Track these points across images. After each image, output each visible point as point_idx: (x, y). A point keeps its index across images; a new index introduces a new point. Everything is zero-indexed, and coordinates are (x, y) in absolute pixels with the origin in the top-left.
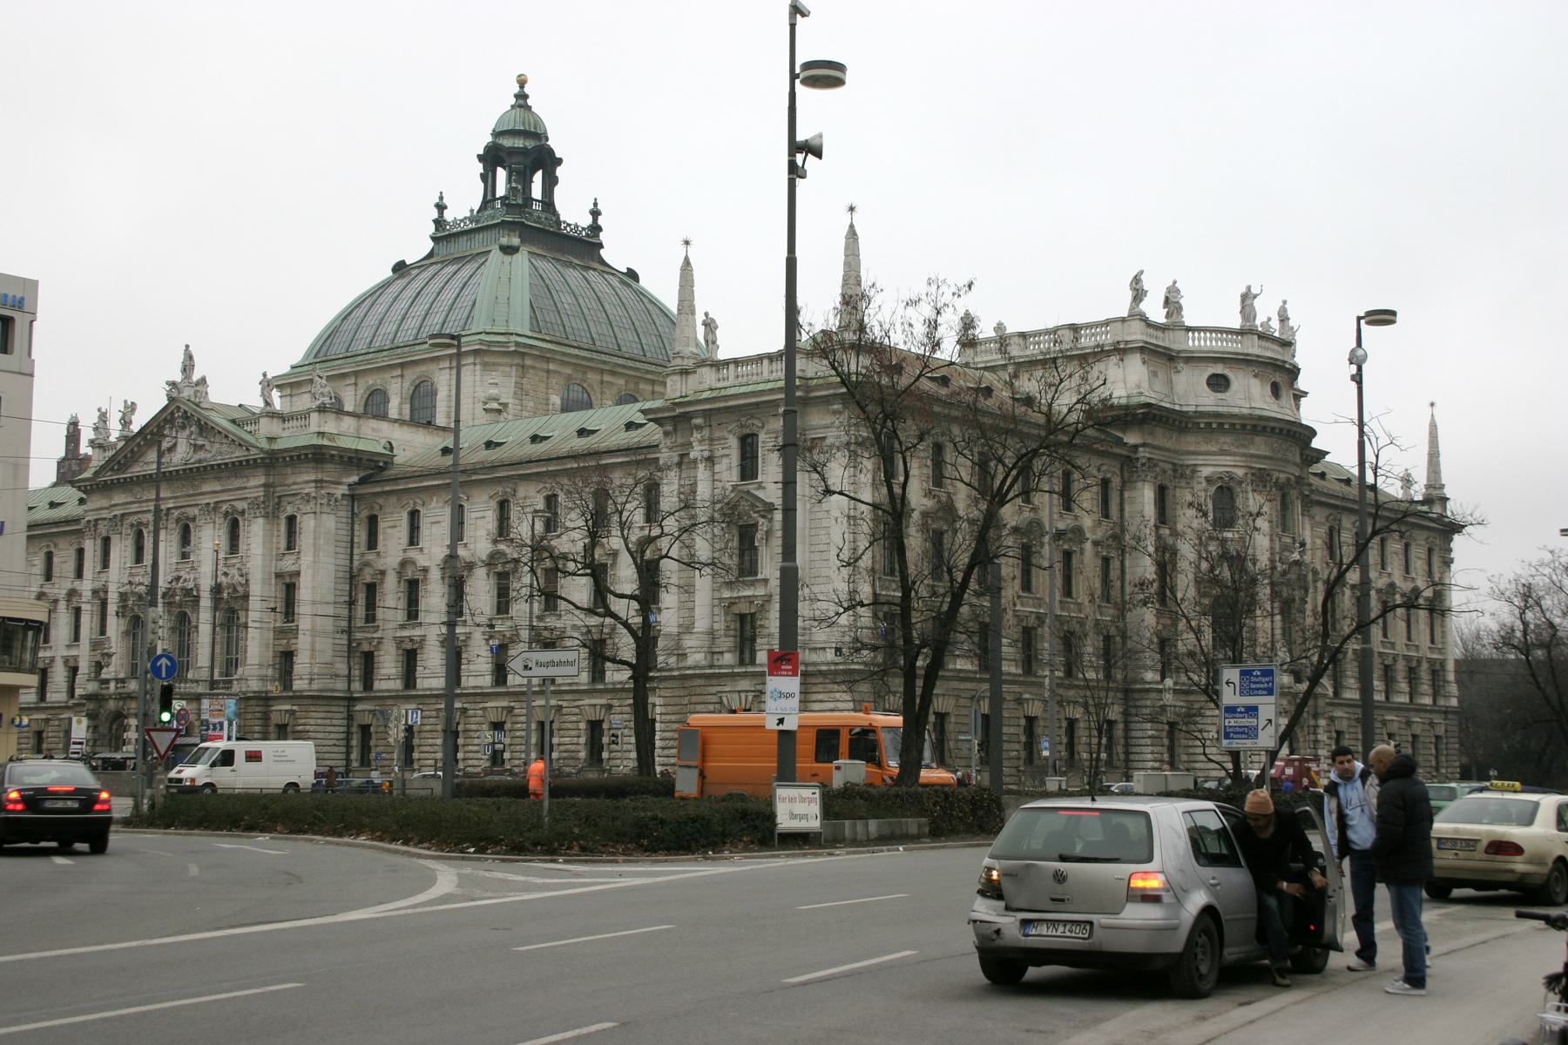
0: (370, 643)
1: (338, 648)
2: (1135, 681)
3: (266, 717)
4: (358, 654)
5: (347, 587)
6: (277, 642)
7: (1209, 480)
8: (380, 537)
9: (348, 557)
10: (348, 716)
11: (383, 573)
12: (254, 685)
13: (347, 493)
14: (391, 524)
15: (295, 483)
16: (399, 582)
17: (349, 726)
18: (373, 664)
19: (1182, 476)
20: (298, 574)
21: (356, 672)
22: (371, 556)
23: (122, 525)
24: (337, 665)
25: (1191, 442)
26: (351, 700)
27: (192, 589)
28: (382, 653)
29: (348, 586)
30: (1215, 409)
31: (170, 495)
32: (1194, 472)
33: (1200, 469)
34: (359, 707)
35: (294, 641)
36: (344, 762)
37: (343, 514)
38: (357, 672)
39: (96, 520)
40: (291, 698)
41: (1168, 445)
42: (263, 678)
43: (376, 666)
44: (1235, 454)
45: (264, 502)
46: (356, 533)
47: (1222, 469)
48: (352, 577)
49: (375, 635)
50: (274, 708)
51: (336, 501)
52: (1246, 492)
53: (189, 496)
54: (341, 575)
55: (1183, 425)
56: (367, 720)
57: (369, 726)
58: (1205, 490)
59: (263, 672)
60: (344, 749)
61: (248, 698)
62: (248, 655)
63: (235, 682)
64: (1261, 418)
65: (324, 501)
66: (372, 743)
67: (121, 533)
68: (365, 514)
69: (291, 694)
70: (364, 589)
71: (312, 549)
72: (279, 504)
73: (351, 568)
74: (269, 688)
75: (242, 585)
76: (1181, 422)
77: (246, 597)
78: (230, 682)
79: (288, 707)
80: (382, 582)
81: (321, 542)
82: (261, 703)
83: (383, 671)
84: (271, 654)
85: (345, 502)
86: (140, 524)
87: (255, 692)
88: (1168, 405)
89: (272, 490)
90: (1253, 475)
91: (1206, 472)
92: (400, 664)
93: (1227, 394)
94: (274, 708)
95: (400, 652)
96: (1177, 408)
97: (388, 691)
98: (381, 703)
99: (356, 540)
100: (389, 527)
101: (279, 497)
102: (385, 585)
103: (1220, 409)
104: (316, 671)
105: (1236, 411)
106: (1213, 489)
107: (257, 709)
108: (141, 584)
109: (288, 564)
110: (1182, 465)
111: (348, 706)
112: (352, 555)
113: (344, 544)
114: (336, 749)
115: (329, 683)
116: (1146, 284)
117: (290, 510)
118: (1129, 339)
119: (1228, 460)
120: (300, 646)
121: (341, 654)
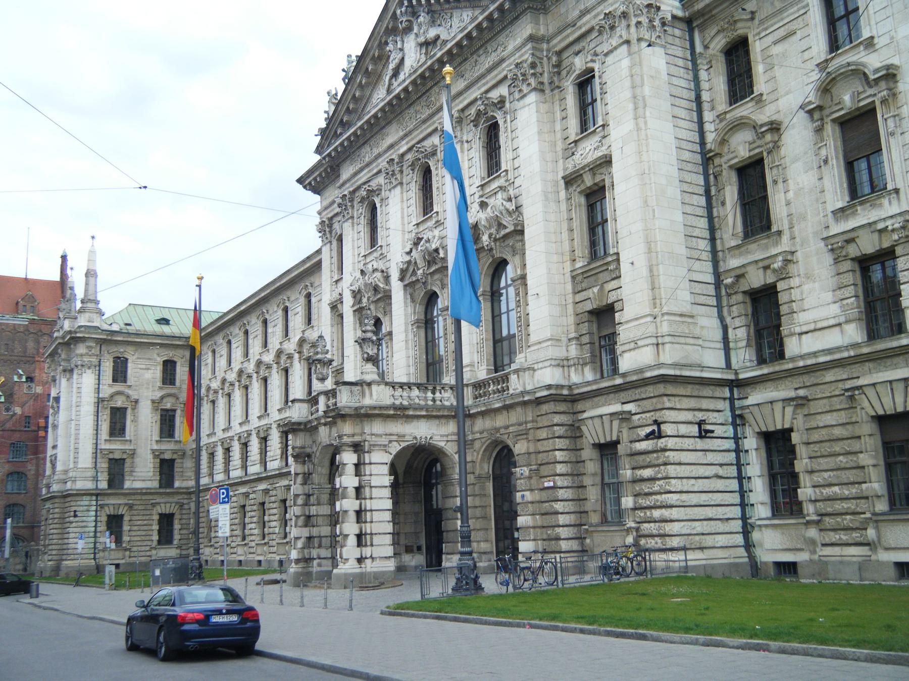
0: (766, 268)
1: (698, 288)
3: (575, 432)
4: (740, 297)
5: (701, 180)
6: (579, 297)
8: (759, 69)
9: (695, 127)
10: (734, 416)
11: (775, 127)
12: (548, 376)
13: (680, 13)
14: (781, 33)
15: (583, 14)
16: (819, 130)
17: (736, 439)
18: (777, 305)
20: (606, 161)
21: (740, 333)
22: (745, 109)
23: (353, 207)
24: (704, 321)
26: (736, 384)
27: (436, 250)
28: (795, 282)
29: (702, 177)
31: (401, 133)
34: (755, 397)
35: (613, 284)
36: (737, 512)
37: (679, 52)
38: (742, 333)
39: (331, 219)
40: (618, 389)
42: (563, 364)
43: (784, 309)
45: (533, 66)
46: (705, 85)
48: (707, 159)
49: (774, 251)
50: (585, 415)
51: (664, 24)
53: (424, 121)
54: (687, 156)
56: (779, 420)
57: (786, 433)
59: (560, 353)
60: (734, 485)
61: (539, 402)
62: (532, 328)
63: (513, 378)
65: (644, 19)
66: (800, 465)
67: (352, 217)
68: (719, 43)
69: (619, 381)
70: (734, 177)
71: (631, 106)
72: (558, 65)
73: (703, 143)
74: (575, 378)
75: (510, 213)
77: (519, 232)
78: (506, 378)
79: (616, 408)
80: (776, 146)
81: (647, 90)
82: (562, 407)
83: (802, 317)
84: (571, 320)
85: (677, 32)
86: (371, 192)
87: (549, 387)
89: (545, 46)
92: (850, 291)
94: (585, 415)
95: (847, 265)
97: (829, 351)
98: (808, 380)
99: (705, 96)
100: (775, 43)
101: (559, 53)
102: (783, 151)
104: (665, 328)
107: (557, 419)
108: (375, 270)
109: (588, 152)
111: (732, 400)
112: (701, 123)
113: (684, 104)
114: (720, 485)
115: (693, 354)
117: (579, 64)
120: (625, 293)
121: (702, 300)
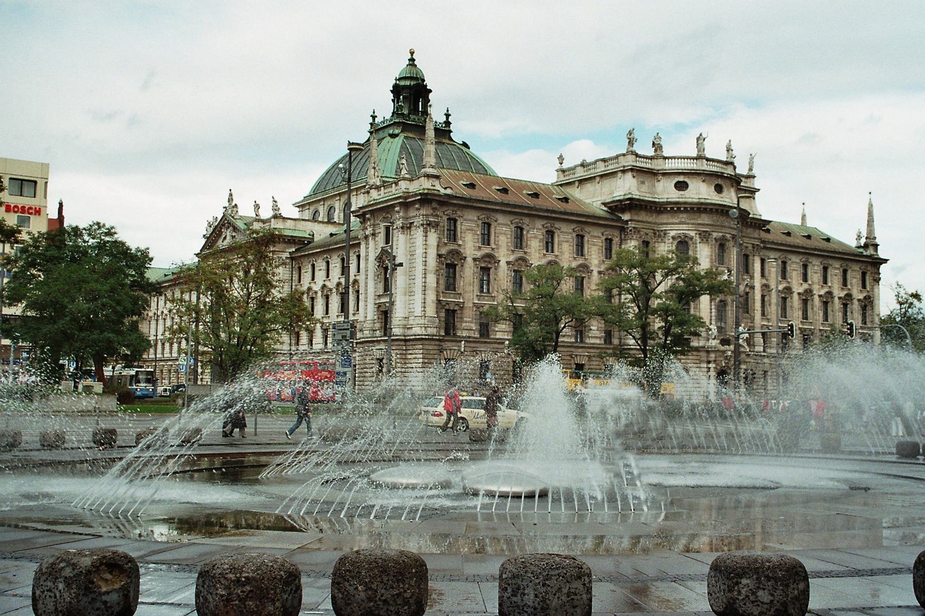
19: (659, 236)
25: (664, 218)
30: (677, 200)
32: (665, 234)
41: (650, 220)
44: (688, 224)
47: (679, 232)
52: (696, 244)
64: (702, 204)
76: (656, 208)
88: (650, 199)
90: (700, 234)
103: (681, 200)
105: (690, 200)
106: (675, 243)
116: (636, 135)
118: (626, 164)
119: (685, 227)
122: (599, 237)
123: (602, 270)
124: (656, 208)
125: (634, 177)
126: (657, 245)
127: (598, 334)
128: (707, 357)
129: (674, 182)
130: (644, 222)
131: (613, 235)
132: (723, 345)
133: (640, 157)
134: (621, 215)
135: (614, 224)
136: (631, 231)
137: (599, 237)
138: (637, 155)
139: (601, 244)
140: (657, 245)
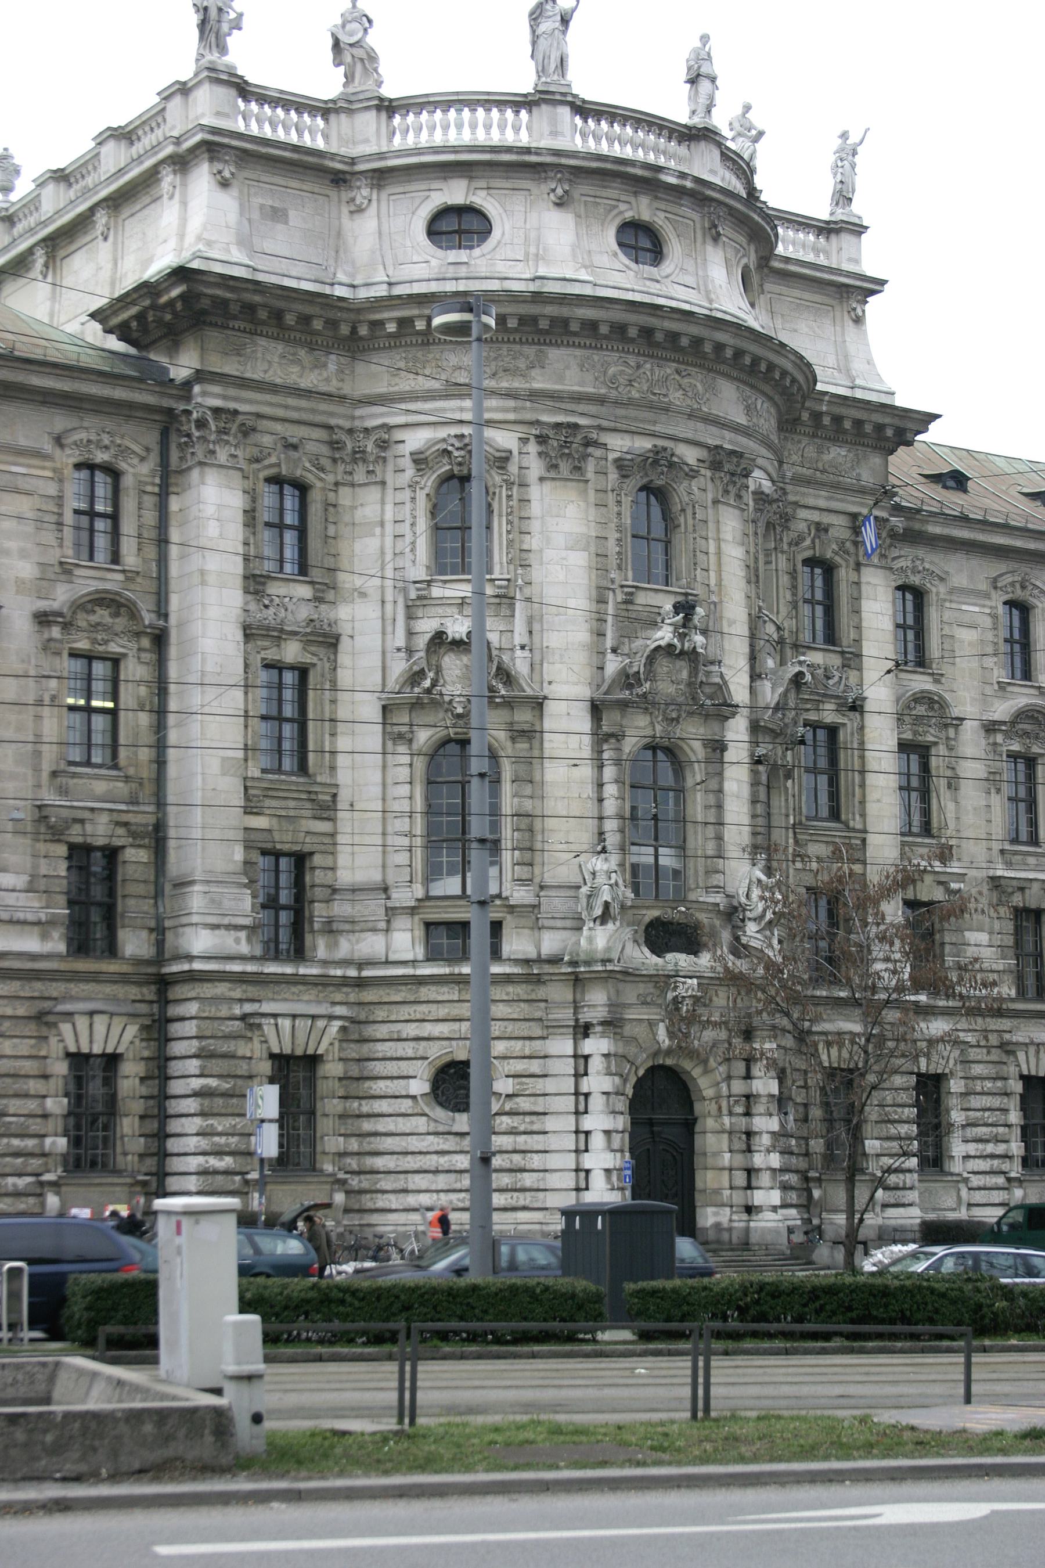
2: (178, 957)
7: (420, 460)
33: (398, 435)
41: (309, 380)
55: (345, 330)
58: (412, 486)
76: (332, 324)
91: (416, 440)
93: (477, 252)
96: (340, 291)
110: (351, 431)
122: (37, 454)
123: (56, 605)
124: (332, 324)
125: (224, 184)
126: (345, 497)
127: (31, 906)
128: (576, 1007)
129: (426, 211)
130: (272, 388)
131: (124, 451)
132: (658, 950)
133: (263, 97)
134: (163, 359)
135: (119, 393)
136: (201, 424)
137: (37, 454)
138: (243, 89)
139: (52, 490)
140: (345, 497)
